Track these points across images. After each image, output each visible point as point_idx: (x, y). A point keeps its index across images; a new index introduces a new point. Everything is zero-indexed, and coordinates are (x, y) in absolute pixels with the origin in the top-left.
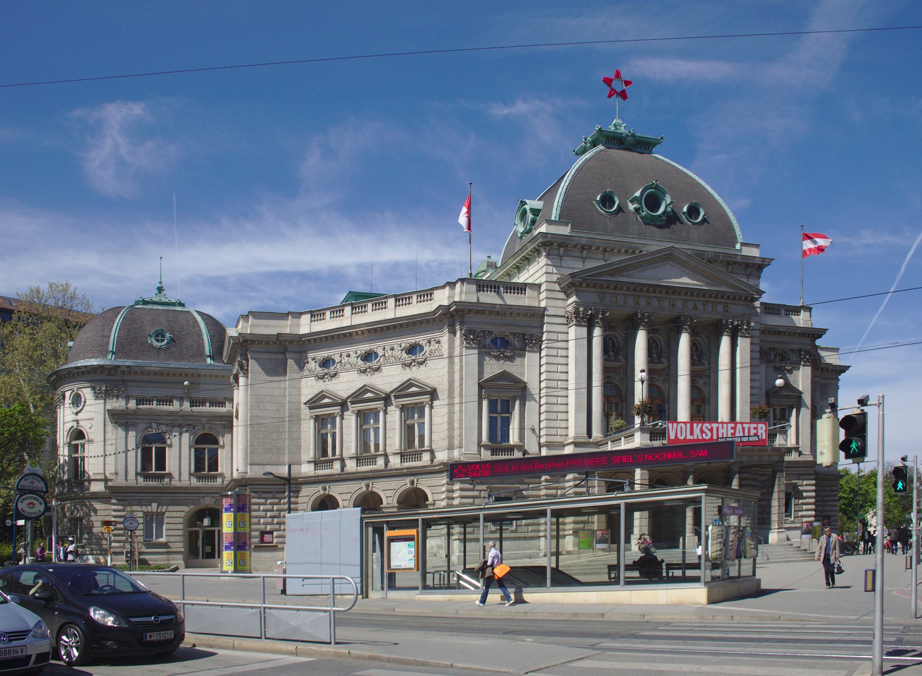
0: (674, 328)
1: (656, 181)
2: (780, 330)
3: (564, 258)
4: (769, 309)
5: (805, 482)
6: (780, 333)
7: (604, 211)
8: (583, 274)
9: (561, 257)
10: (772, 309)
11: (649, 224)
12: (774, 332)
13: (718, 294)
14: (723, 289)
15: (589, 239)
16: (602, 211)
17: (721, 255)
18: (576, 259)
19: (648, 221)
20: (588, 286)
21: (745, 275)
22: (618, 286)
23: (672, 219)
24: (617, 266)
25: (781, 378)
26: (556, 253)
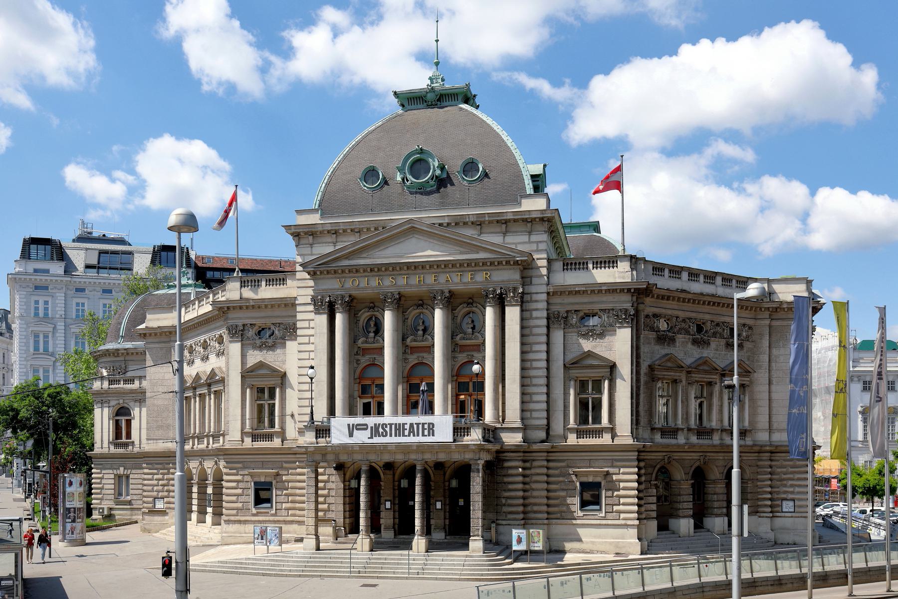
0: (424, 303)
1: (418, 146)
2: (577, 289)
3: (315, 245)
4: (580, 263)
5: (622, 470)
6: (577, 292)
7: (367, 187)
8: (313, 263)
9: (311, 245)
10: (580, 263)
11: (416, 193)
12: (570, 293)
13: (469, 263)
14: (482, 255)
15: (333, 225)
16: (365, 188)
17: (486, 215)
18: (327, 245)
19: (422, 190)
20: (321, 273)
21: (526, 231)
22: (355, 270)
23: (443, 182)
24: (351, 250)
25: (478, 363)
26: (307, 242)
